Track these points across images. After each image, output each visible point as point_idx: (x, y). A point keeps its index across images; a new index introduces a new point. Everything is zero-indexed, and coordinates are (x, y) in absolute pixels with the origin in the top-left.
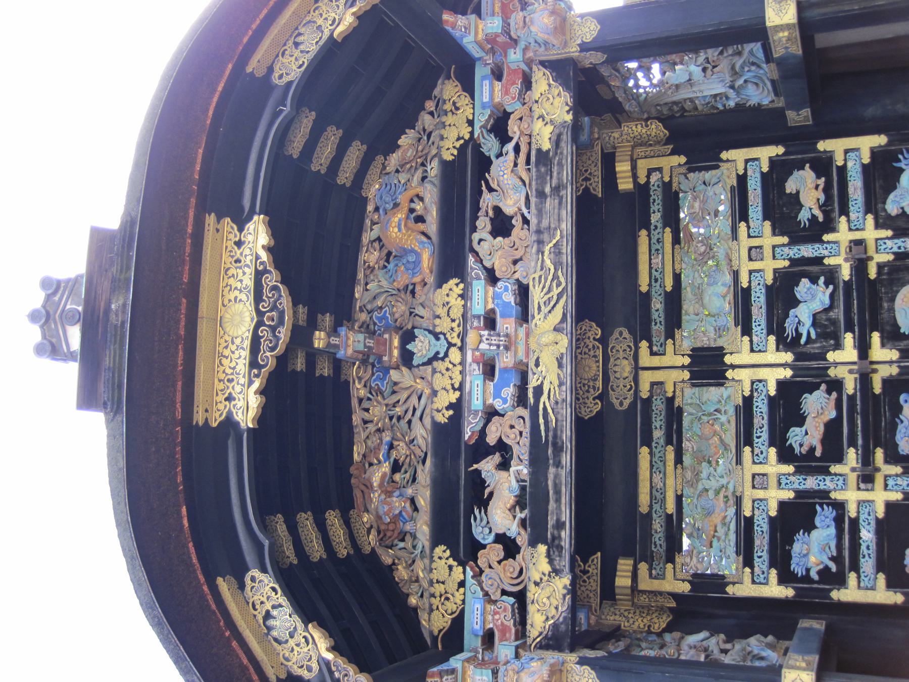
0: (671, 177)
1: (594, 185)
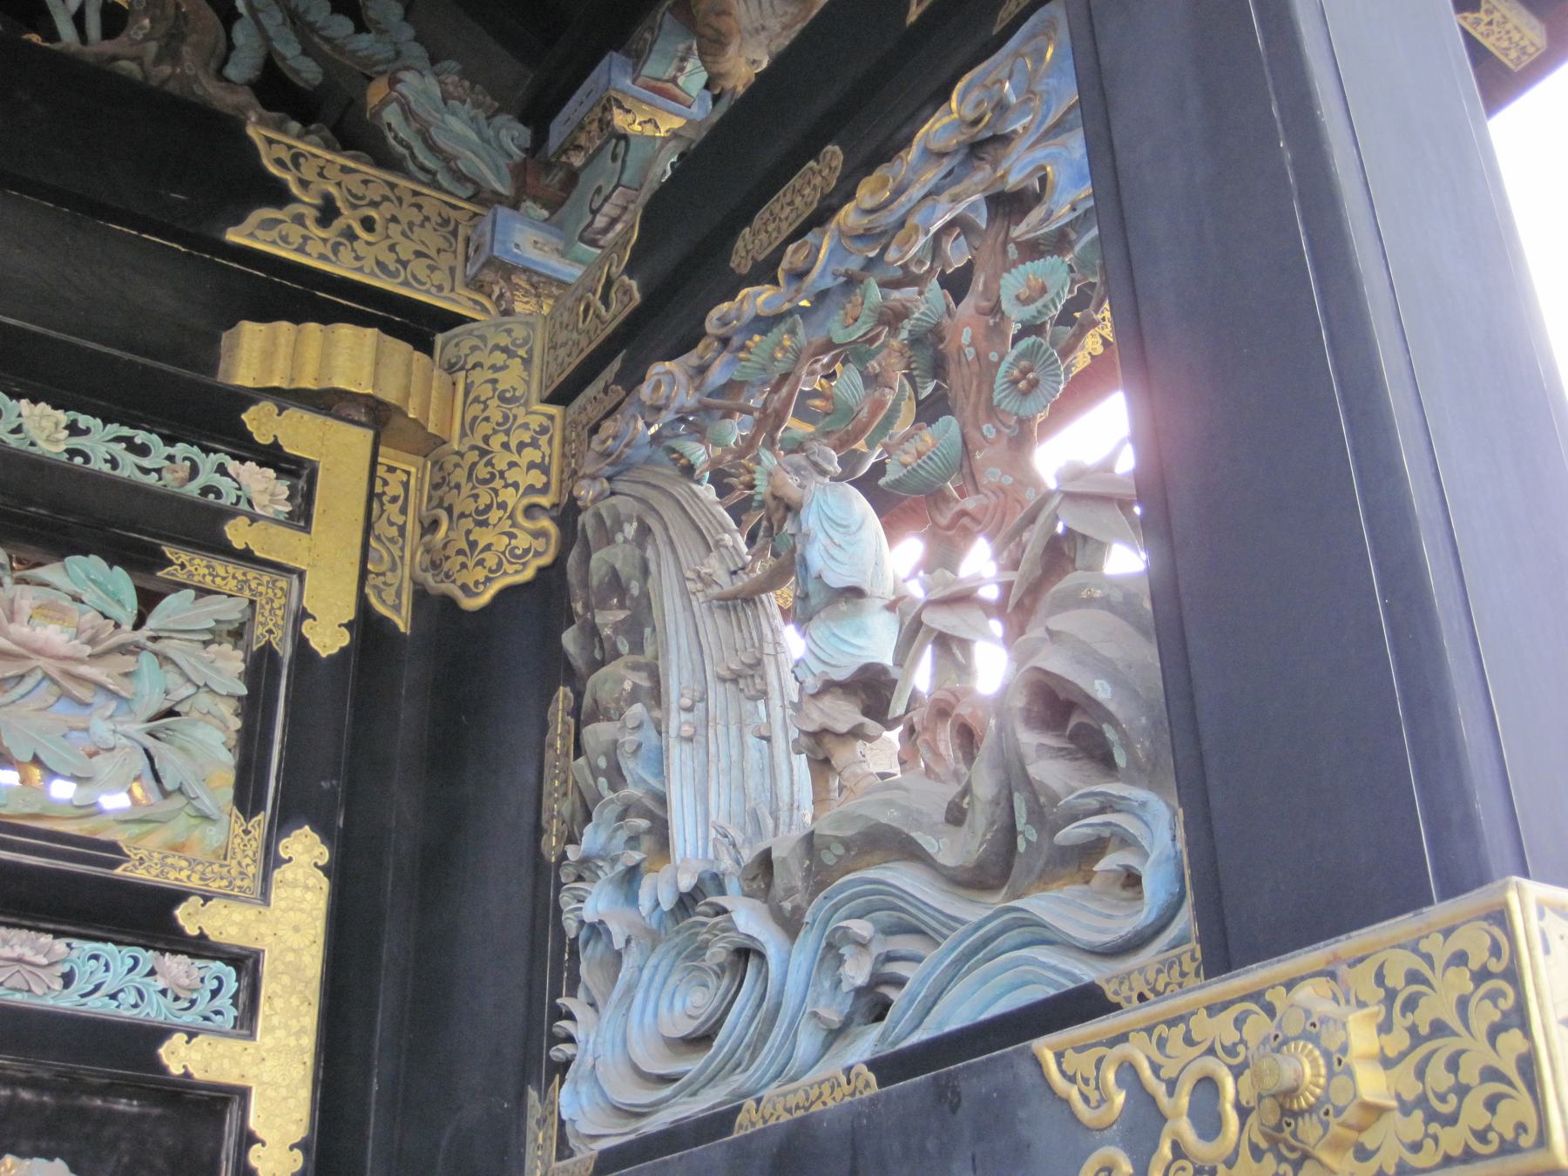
0: (246, 557)
1: (295, 233)
